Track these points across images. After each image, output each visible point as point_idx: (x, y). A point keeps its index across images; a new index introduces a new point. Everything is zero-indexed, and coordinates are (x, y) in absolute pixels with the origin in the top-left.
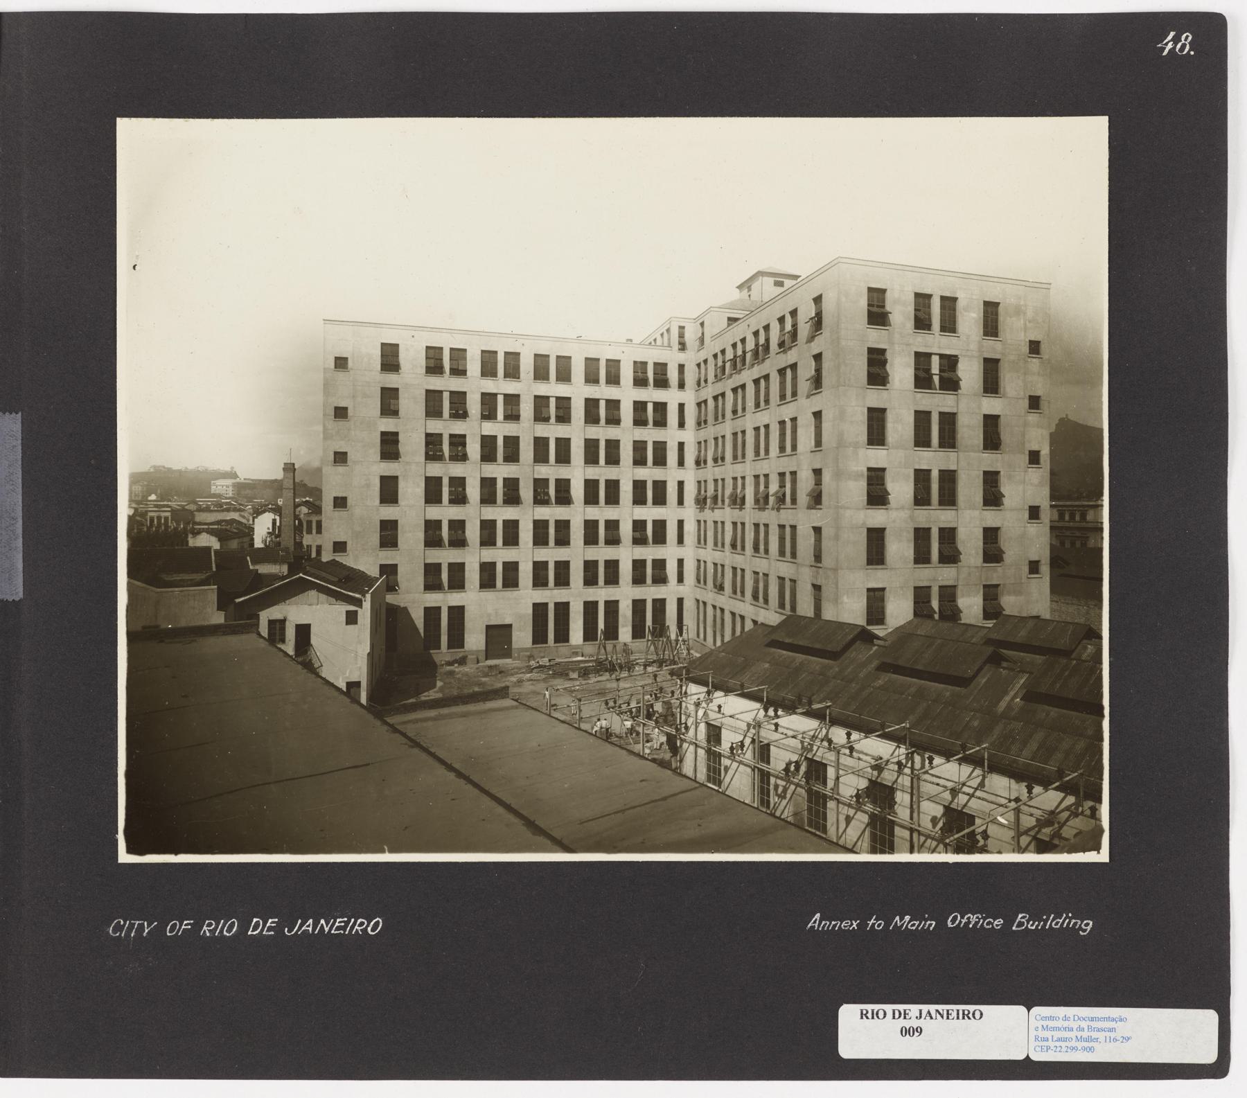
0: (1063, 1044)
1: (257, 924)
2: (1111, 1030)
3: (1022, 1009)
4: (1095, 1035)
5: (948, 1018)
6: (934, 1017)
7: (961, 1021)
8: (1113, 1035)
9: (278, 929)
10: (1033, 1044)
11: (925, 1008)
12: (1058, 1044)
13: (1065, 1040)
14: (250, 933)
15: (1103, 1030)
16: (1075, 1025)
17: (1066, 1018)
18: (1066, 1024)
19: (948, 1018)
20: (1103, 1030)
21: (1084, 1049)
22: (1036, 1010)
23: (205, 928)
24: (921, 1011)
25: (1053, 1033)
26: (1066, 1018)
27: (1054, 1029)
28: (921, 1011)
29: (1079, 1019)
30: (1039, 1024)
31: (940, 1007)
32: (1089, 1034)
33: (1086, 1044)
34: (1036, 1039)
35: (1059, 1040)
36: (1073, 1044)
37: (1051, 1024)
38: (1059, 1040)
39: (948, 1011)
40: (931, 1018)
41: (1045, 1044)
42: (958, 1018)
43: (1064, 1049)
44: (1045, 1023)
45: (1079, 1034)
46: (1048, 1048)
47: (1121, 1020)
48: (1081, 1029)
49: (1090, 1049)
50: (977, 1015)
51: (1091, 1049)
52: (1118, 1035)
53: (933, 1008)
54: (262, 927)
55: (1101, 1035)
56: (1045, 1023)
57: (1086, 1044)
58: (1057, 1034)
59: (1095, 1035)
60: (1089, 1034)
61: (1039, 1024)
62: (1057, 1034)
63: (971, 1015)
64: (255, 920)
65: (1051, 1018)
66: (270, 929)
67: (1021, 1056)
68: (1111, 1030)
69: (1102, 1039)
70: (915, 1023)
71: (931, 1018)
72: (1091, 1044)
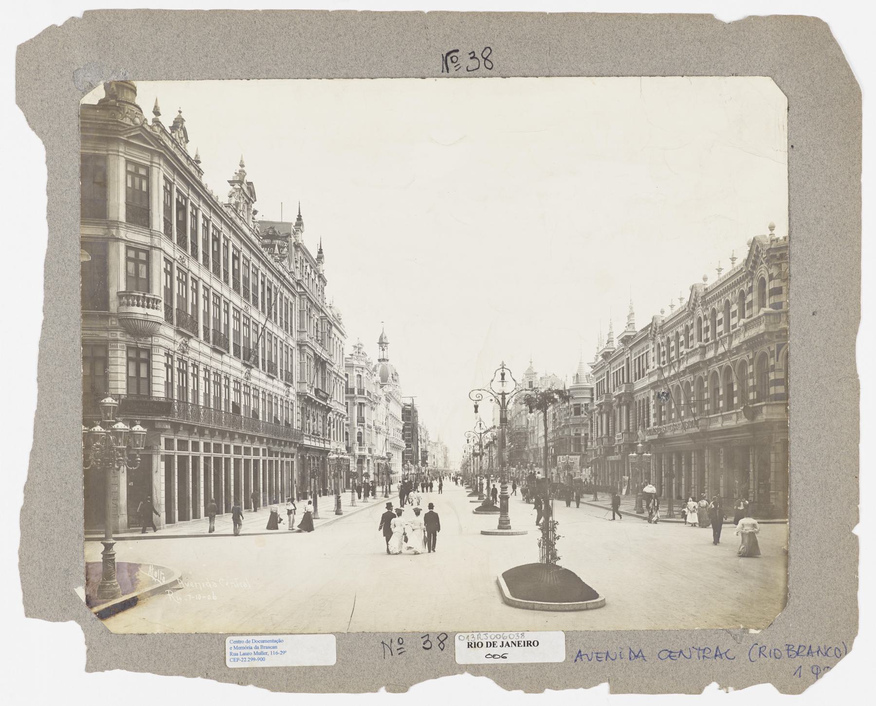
0: (246, 656)
2: (275, 647)
4: (265, 650)
8: (275, 650)
12: (244, 657)
13: (248, 654)
15: (269, 648)
16: (253, 645)
18: (248, 645)
20: (269, 648)
21: (259, 659)
26: (248, 642)
27: (241, 648)
30: (232, 645)
32: (263, 650)
34: (231, 654)
35: (244, 654)
36: (253, 656)
37: (239, 645)
38: (244, 654)
41: (236, 657)
43: (247, 660)
44: (236, 645)
45: (256, 651)
46: (238, 659)
48: (257, 648)
49: (263, 659)
51: (263, 659)
52: (278, 650)
55: (269, 651)
56: (236, 645)
58: (243, 651)
59: (265, 650)
61: (232, 645)
62: (243, 651)
65: (239, 642)
68: (275, 647)
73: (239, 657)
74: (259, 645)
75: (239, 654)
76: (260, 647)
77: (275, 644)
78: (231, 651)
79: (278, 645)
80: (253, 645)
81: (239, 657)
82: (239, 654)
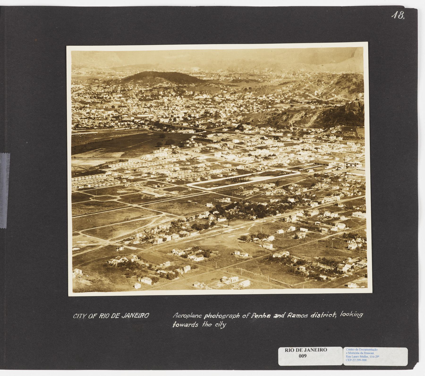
1: (114, 315)
2: (372, 353)
3: (340, 348)
4: (367, 355)
5: (315, 351)
6: (310, 351)
7: (319, 352)
8: (373, 355)
9: (120, 317)
10: (345, 358)
11: (307, 348)
12: (354, 358)
13: (356, 357)
14: (112, 317)
16: (360, 352)
17: (357, 350)
18: (357, 351)
19: (315, 351)
21: (363, 360)
22: (345, 348)
23: (101, 315)
24: (306, 348)
25: (352, 355)
27: (353, 353)
28: (306, 348)
29: (361, 350)
31: (312, 348)
32: (365, 355)
33: (364, 358)
34: (347, 356)
35: (354, 357)
36: (359, 358)
37: (352, 351)
39: (315, 349)
40: (309, 351)
41: (350, 358)
42: (318, 351)
43: (356, 360)
45: (361, 355)
46: (351, 360)
47: (376, 350)
48: (362, 353)
50: (325, 350)
51: (365, 360)
52: (375, 355)
53: (310, 348)
54: (116, 316)
55: (369, 355)
56: (350, 351)
57: (364, 358)
58: (354, 355)
59: (367, 355)
60: (365, 355)
63: (323, 350)
64: (113, 314)
66: (118, 316)
67: (341, 364)
68: (372, 353)
69: (369, 357)
70: (304, 353)
71: (309, 351)
72: (365, 358)
73: (351, 358)
74: (363, 352)
75: (351, 357)
76: (364, 353)
77: (372, 352)
78: (347, 355)
79: (375, 352)
80: (360, 352)
81: (351, 358)
82: (351, 357)
